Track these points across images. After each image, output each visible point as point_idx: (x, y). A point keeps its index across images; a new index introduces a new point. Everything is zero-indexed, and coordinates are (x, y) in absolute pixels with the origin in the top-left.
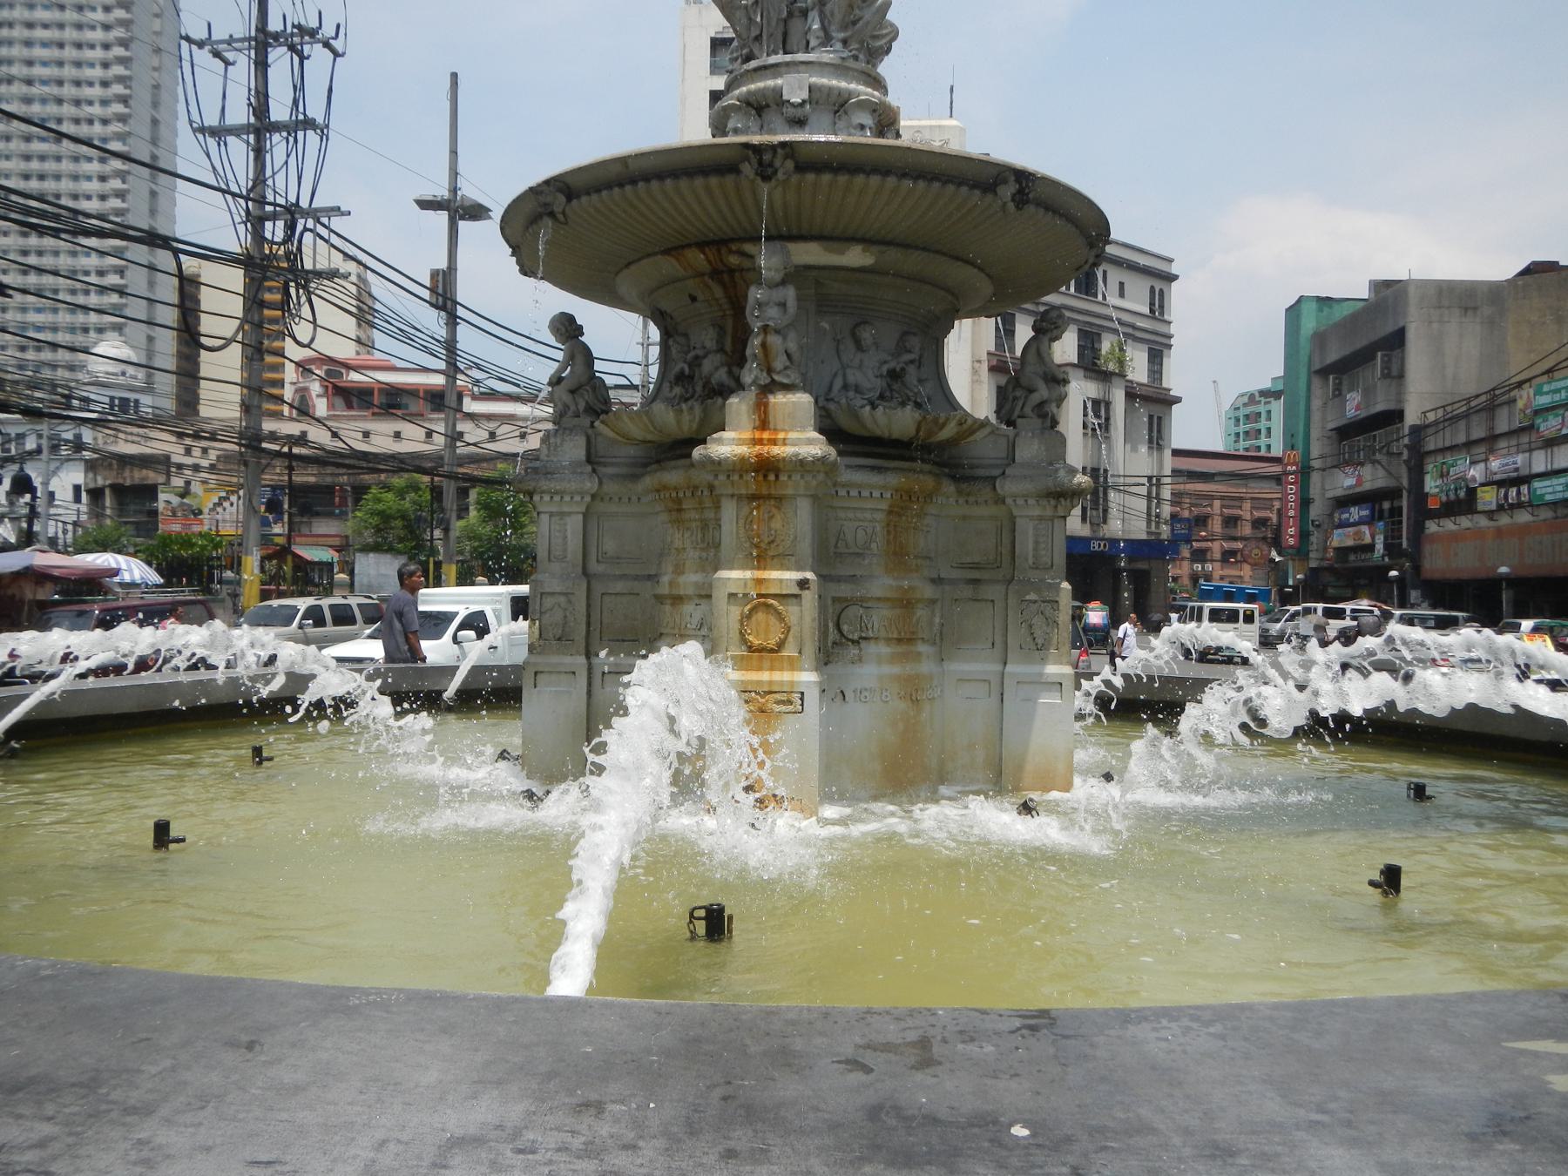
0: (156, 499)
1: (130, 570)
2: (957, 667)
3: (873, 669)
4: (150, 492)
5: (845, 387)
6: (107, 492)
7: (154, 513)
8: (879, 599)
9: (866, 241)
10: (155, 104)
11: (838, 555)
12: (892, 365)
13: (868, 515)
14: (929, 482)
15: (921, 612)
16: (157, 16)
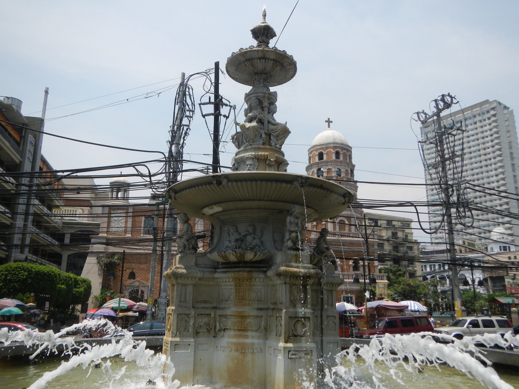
0: (504, 281)
1: (414, 306)
2: (269, 342)
3: (228, 340)
4: (502, 279)
5: (226, 248)
6: (489, 279)
7: (504, 286)
8: (230, 315)
9: (215, 203)
10: (510, 148)
11: (222, 300)
12: (237, 238)
13: (229, 287)
14: (245, 275)
15: (248, 320)
16: (506, 121)
